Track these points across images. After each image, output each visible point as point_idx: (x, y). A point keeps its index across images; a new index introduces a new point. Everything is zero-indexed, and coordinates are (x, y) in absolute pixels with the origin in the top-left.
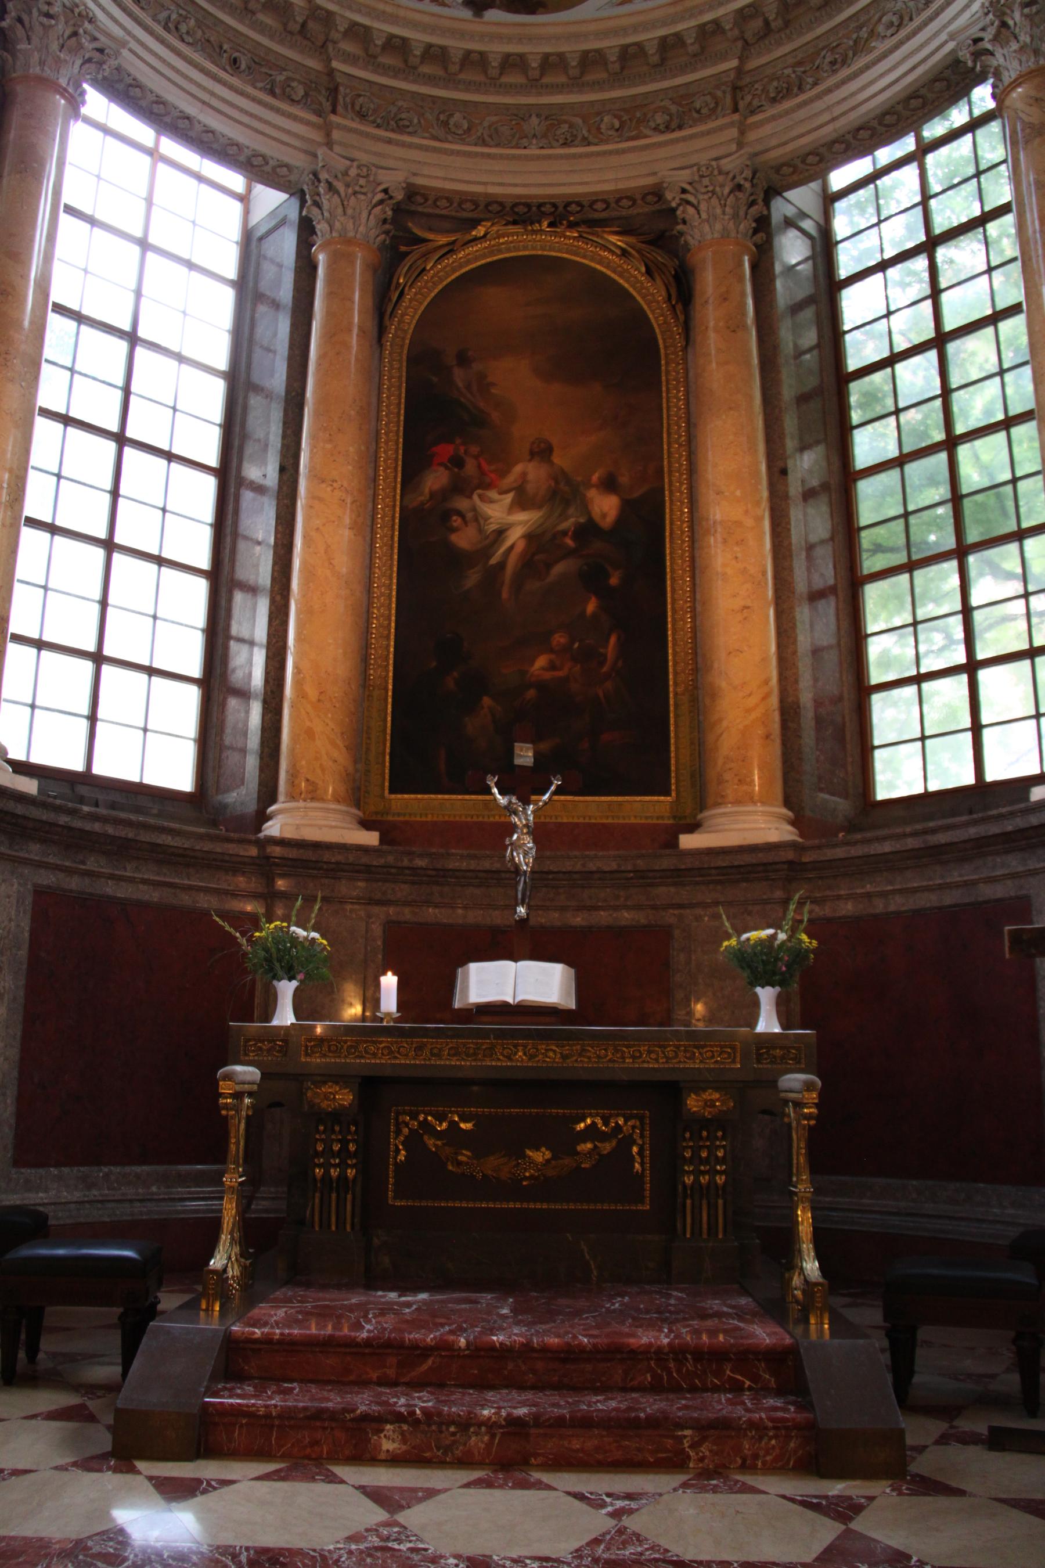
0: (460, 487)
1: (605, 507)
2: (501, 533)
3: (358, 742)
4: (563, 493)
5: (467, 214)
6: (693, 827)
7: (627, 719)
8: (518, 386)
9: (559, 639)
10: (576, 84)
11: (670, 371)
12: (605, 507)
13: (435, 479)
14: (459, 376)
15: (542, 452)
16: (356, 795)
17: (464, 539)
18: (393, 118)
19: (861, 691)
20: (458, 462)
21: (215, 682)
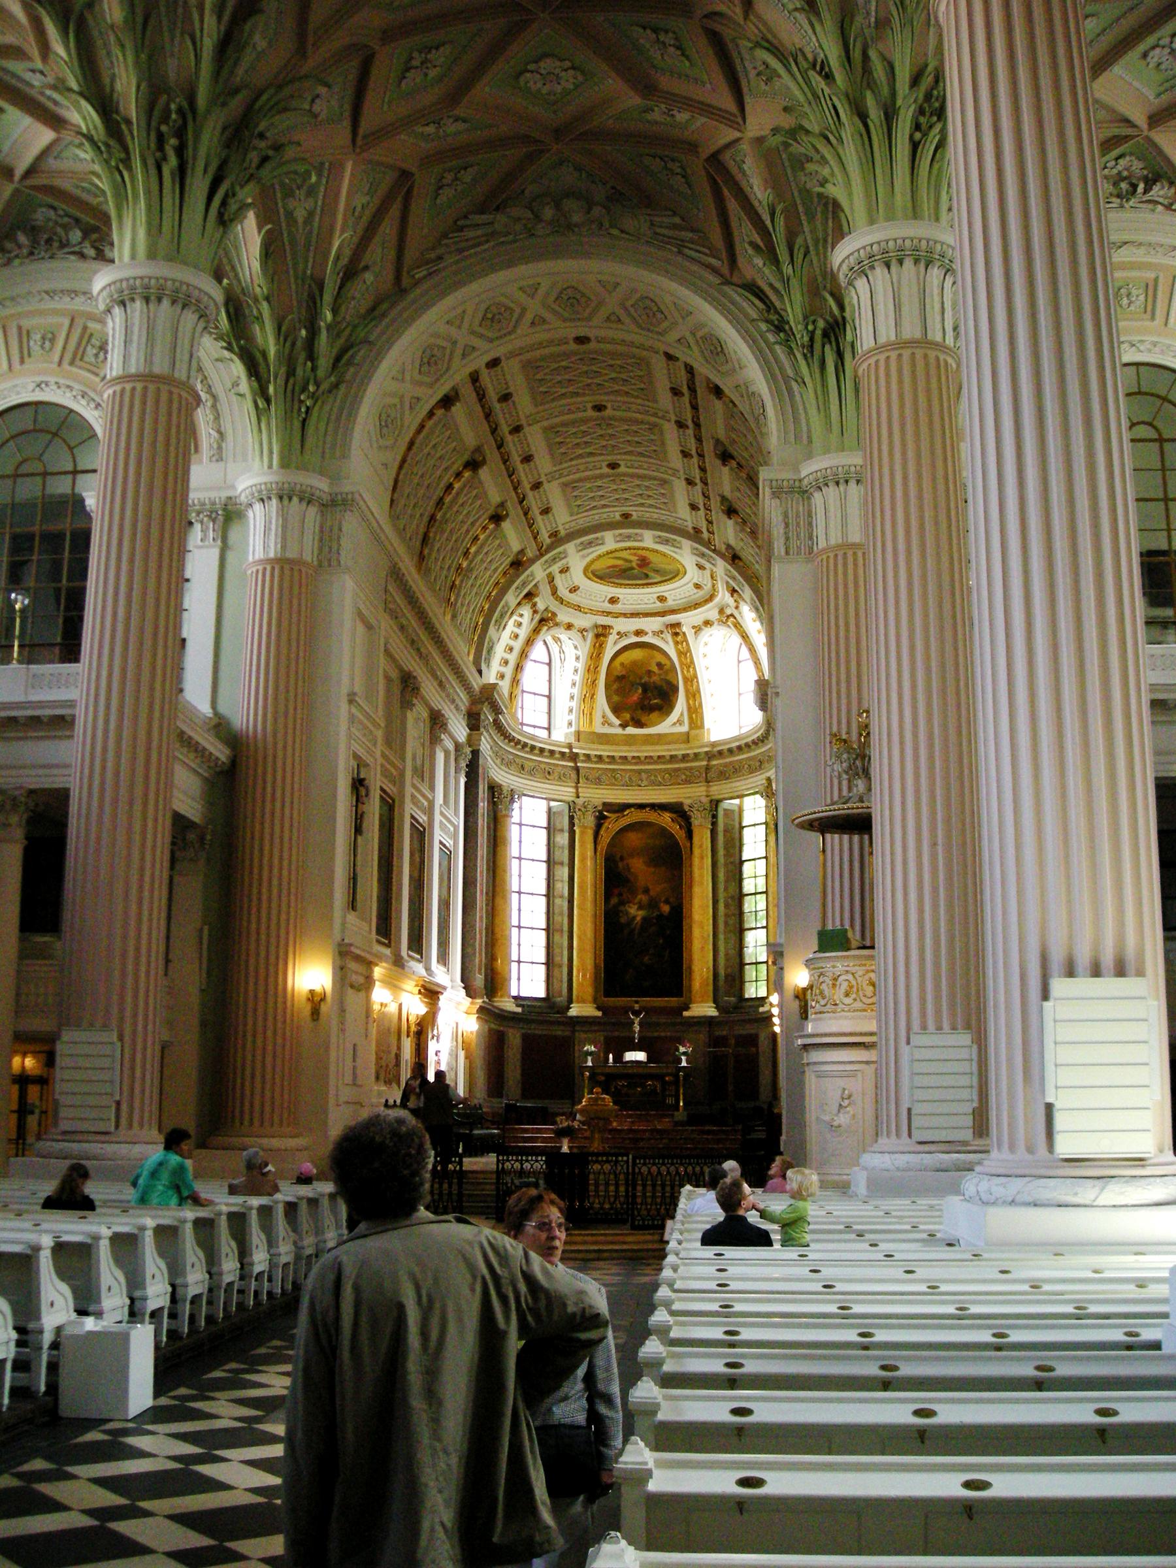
0: (622, 903)
1: (666, 909)
2: (634, 917)
3: (596, 989)
4: (653, 904)
5: (622, 808)
6: (687, 1008)
7: (670, 975)
8: (638, 866)
9: (651, 951)
10: (656, 763)
11: (685, 863)
12: (666, 909)
13: (614, 900)
14: (620, 865)
15: (646, 891)
16: (595, 1000)
17: (623, 920)
18: (598, 781)
19: (742, 965)
20: (621, 894)
21: (549, 963)
